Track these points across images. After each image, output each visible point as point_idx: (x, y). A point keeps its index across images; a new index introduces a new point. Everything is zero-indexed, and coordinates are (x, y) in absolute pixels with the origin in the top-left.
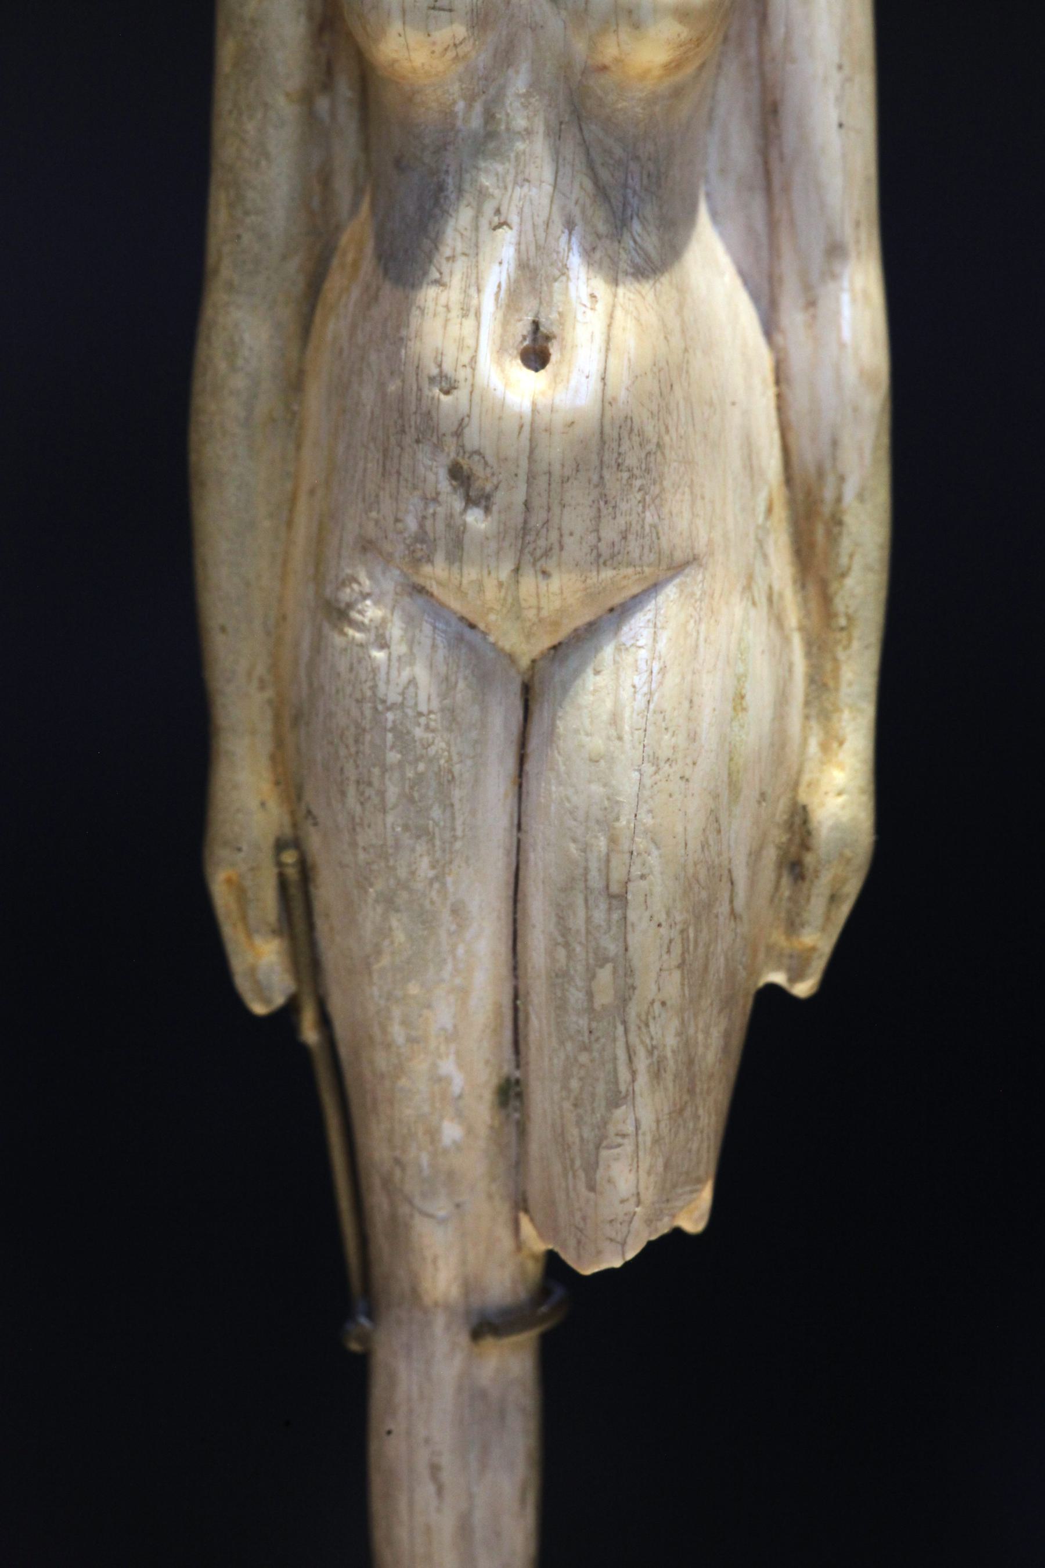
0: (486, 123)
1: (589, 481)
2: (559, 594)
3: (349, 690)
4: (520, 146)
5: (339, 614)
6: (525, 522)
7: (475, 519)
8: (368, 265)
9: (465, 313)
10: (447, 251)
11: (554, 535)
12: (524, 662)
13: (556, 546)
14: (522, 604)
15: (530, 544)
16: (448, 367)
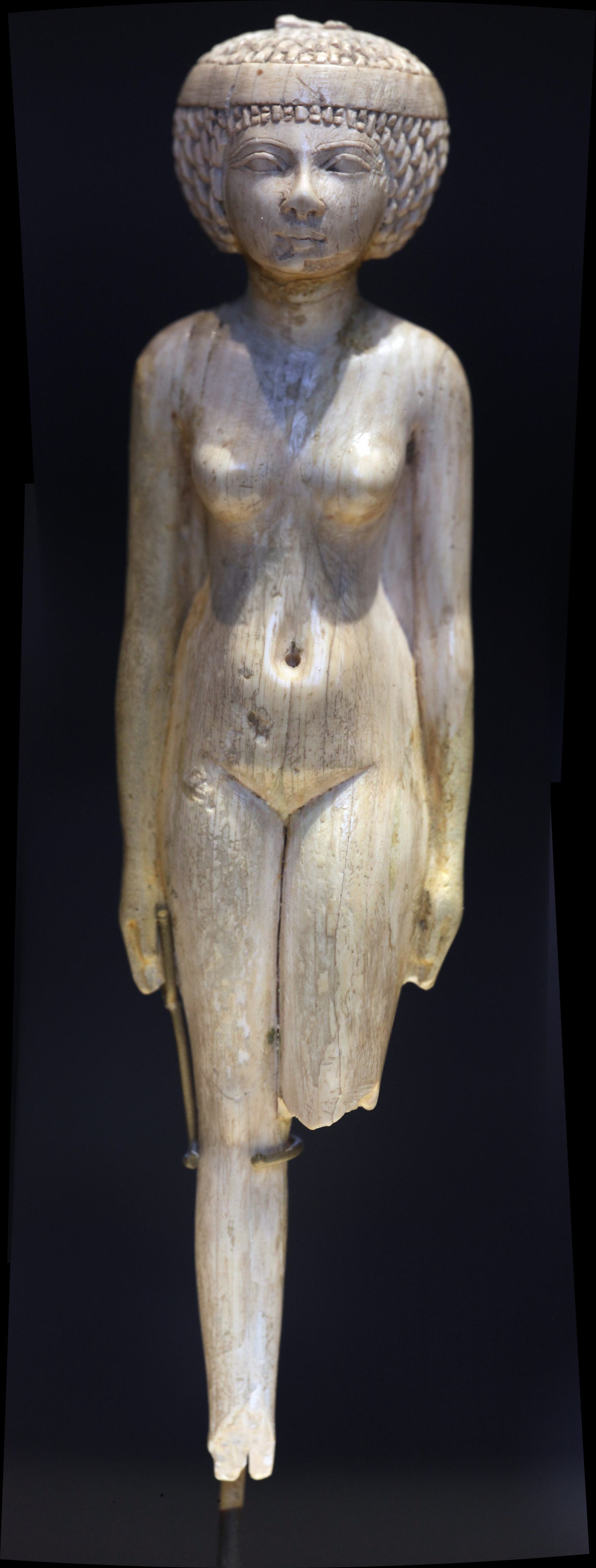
3: (194, 828)
11: (301, 751)
12: (285, 816)
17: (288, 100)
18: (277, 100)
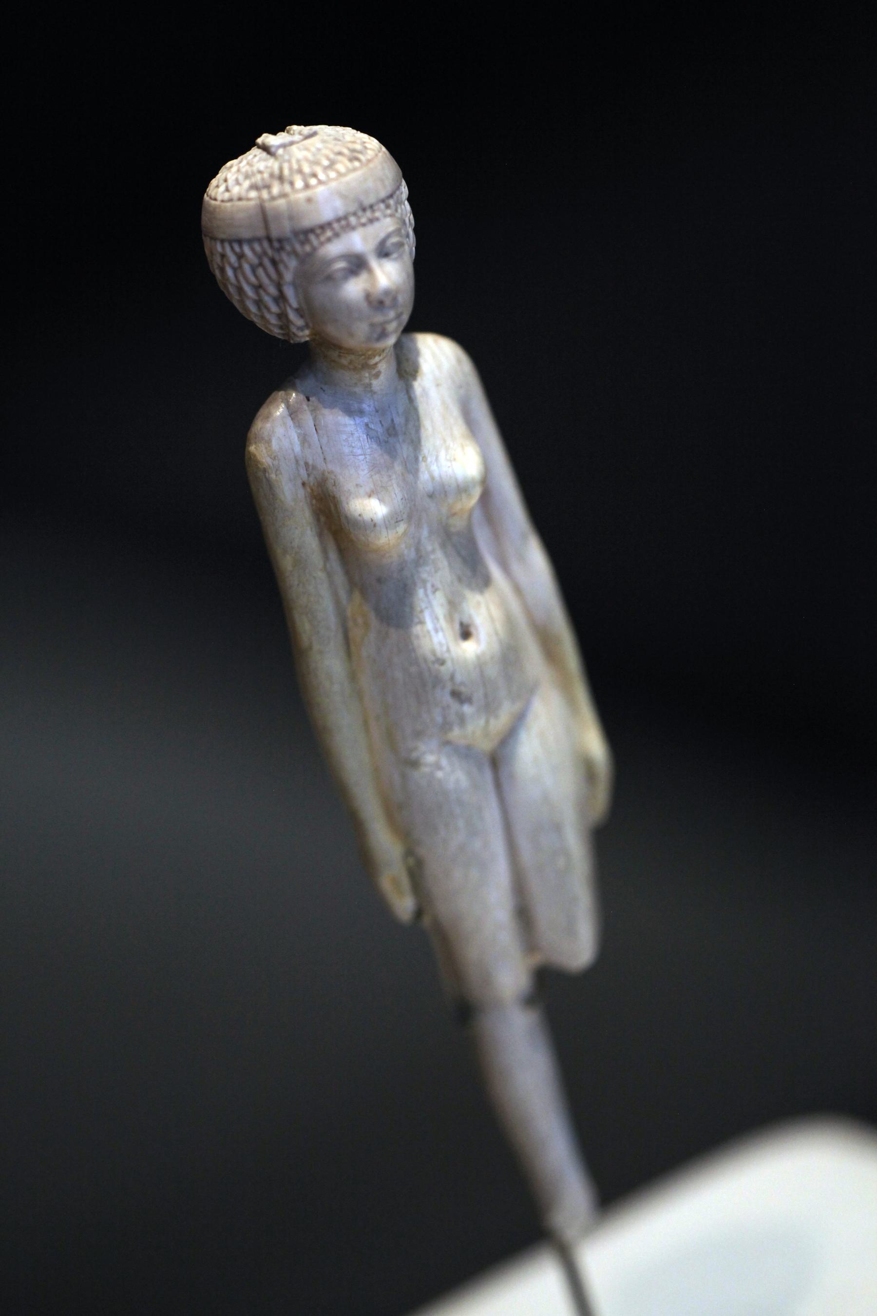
0: (417, 554)
2: (501, 722)
4: (432, 557)
5: (415, 764)
7: (467, 709)
8: (374, 622)
9: (436, 631)
10: (418, 609)
14: (478, 729)
15: (489, 707)
16: (439, 654)
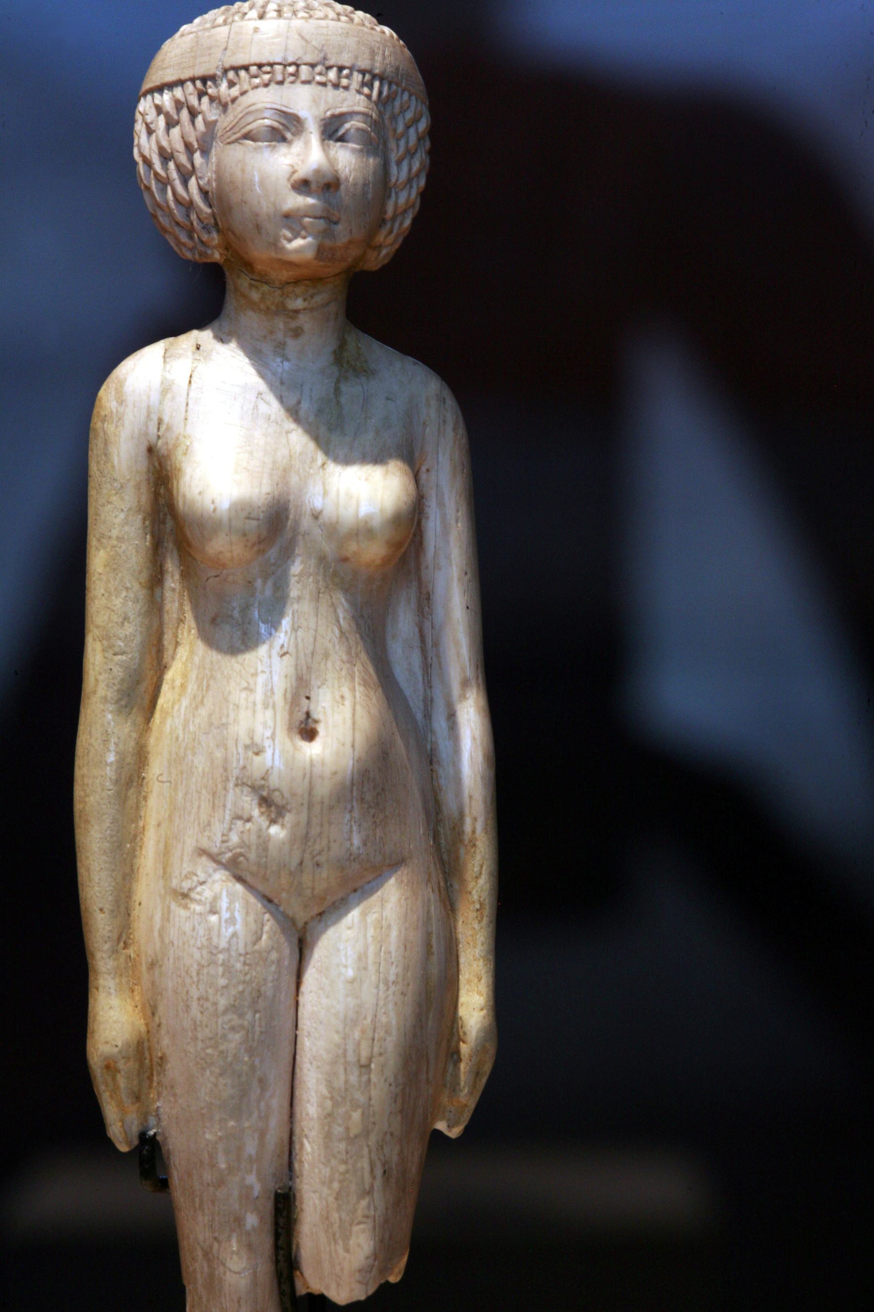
0: (274, 592)
1: (346, 808)
3: (192, 942)
4: (296, 606)
6: (307, 833)
9: (266, 706)
11: (324, 842)
12: (300, 924)
13: (326, 849)
16: (257, 739)
17: (291, 59)
18: (278, 59)
